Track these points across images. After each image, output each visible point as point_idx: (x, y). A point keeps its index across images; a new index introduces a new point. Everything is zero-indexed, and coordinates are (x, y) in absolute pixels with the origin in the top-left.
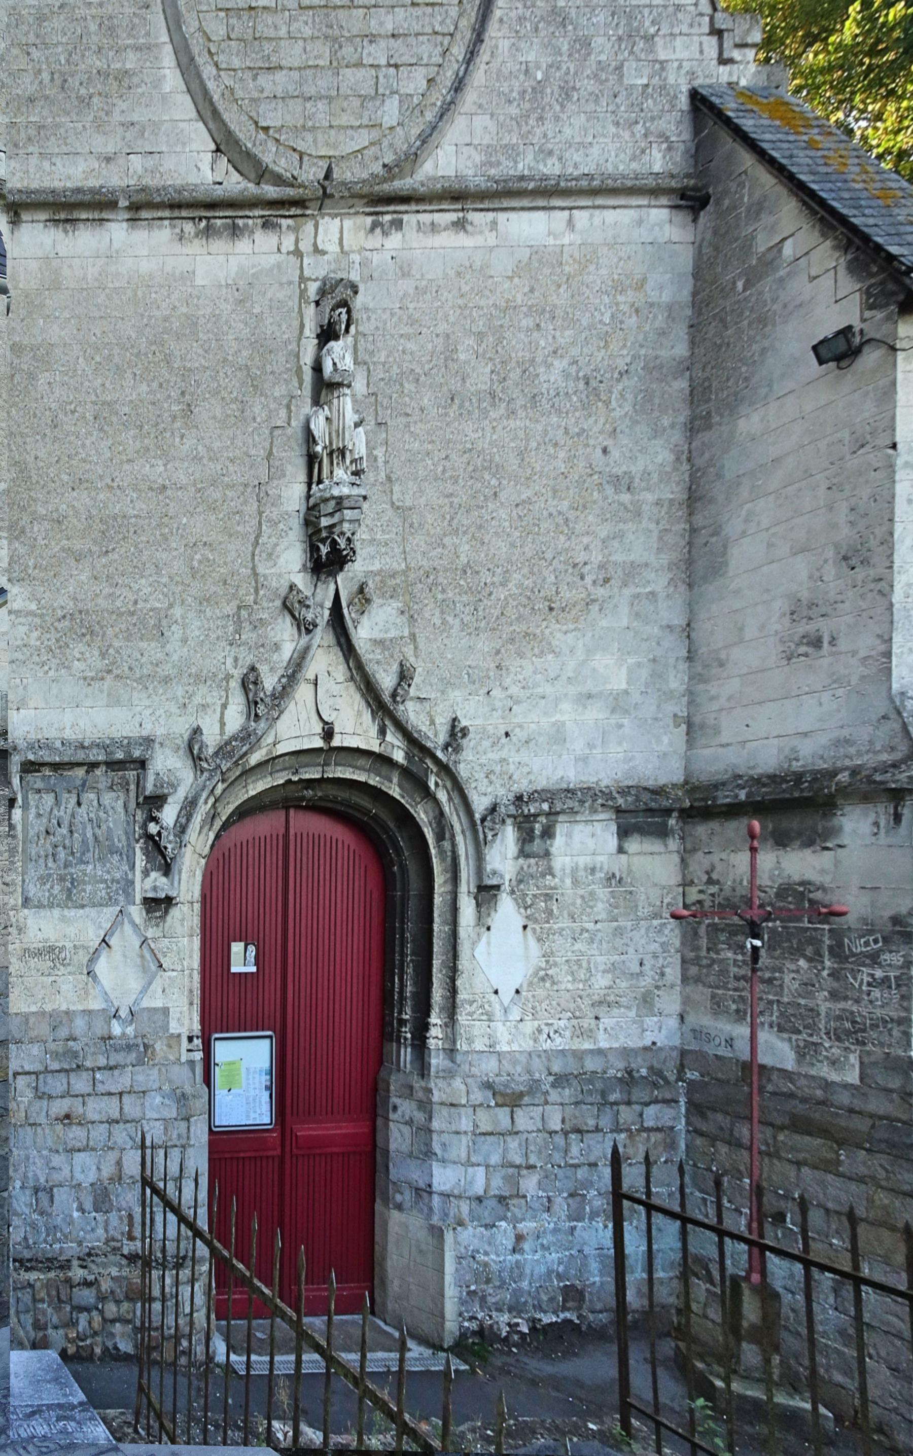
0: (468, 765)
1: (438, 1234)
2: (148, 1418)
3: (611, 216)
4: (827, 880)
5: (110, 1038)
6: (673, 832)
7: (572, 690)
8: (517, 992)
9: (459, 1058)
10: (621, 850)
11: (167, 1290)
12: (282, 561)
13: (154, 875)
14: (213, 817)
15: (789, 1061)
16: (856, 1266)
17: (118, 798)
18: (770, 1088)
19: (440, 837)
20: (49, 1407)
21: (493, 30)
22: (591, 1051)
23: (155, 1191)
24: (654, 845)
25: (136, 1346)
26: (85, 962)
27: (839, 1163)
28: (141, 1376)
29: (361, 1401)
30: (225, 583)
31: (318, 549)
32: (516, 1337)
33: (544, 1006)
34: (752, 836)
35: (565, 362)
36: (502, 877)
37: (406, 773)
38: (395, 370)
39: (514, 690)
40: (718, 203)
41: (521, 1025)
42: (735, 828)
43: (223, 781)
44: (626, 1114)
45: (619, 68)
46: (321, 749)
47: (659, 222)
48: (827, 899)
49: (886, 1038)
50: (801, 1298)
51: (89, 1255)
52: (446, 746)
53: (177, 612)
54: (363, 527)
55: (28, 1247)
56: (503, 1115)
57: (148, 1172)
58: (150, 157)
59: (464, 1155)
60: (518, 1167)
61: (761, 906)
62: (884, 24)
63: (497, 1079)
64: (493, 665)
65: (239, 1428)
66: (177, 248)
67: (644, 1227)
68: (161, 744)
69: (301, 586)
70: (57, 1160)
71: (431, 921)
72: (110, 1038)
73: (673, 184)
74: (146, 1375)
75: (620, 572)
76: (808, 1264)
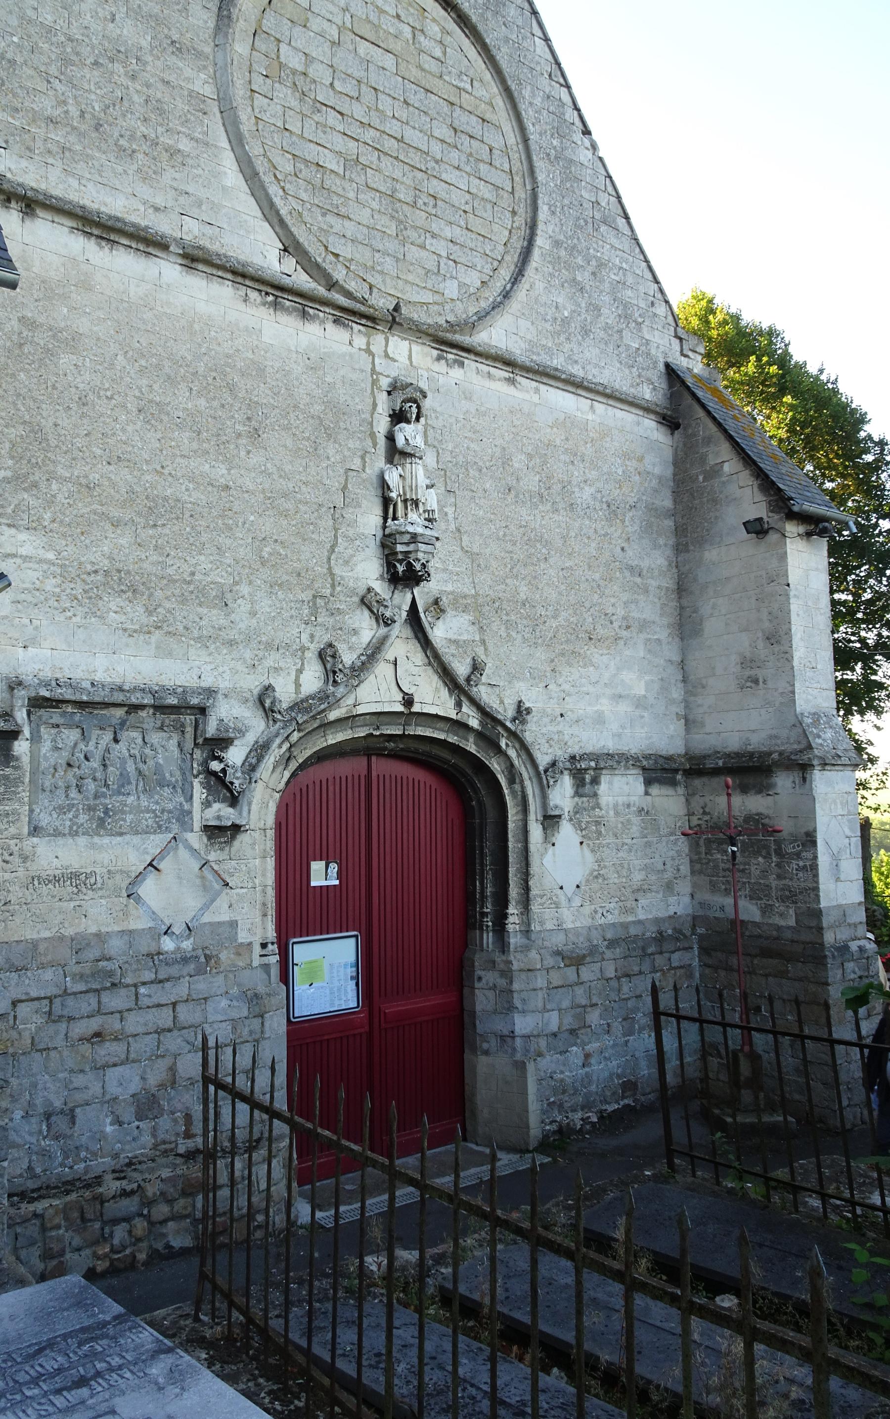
0: (531, 733)
1: (521, 1066)
2: (213, 1302)
3: (620, 414)
4: (770, 812)
5: (159, 953)
6: (680, 783)
7: (608, 691)
8: (578, 886)
9: (533, 937)
10: (647, 793)
11: (237, 1174)
12: (359, 568)
13: (216, 806)
14: (289, 759)
15: (758, 918)
16: (802, 1030)
17: (170, 737)
18: (747, 933)
19: (511, 781)
20: (65, 1337)
21: (530, 272)
22: (634, 922)
23: (220, 1086)
24: (669, 791)
25: (196, 1238)
26: (124, 885)
27: (788, 972)
28: (203, 1264)
29: (456, 1212)
30: (299, 575)
31: (395, 566)
32: (588, 1127)
33: (598, 895)
34: (728, 787)
35: (593, 490)
36: (562, 809)
37: (481, 736)
38: (461, 459)
39: (566, 687)
40: (685, 429)
41: (581, 909)
42: (718, 782)
43: (299, 730)
44: (660, 960)
45: (620, 331)
46: (402, 713)
47: (649, 426)
48: (771, 823)
49: (807, 899)
50: (773, 1055)
51: (130, 1164)
52: (514, 720)
53: (245, 589)
54: (436, 558)
55: (35, 1176)
56: (571, 973)
57: (212, 1070)
58: (209, 226)
59: (540, 1005)
60: (585, 1007)
61: (735, 827)
62: (768, 373)
63: (565, 948)
64: (548, 669)
65: (327, 1276)
66: (242, 306)
67: (676, 1031)
68: (226, 696)
69: (378, 590)
70: (79, 1080)
71: (505, 840)
72: (159, 953)
73: (658, 409)
74: (209, 1261)
75: (637, 624)
76: (775, 1033)
